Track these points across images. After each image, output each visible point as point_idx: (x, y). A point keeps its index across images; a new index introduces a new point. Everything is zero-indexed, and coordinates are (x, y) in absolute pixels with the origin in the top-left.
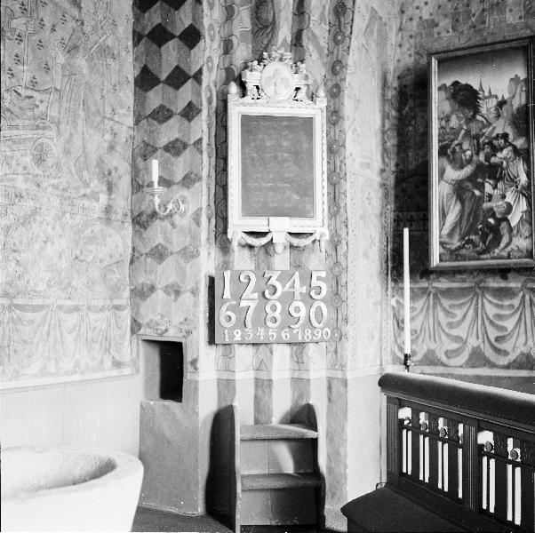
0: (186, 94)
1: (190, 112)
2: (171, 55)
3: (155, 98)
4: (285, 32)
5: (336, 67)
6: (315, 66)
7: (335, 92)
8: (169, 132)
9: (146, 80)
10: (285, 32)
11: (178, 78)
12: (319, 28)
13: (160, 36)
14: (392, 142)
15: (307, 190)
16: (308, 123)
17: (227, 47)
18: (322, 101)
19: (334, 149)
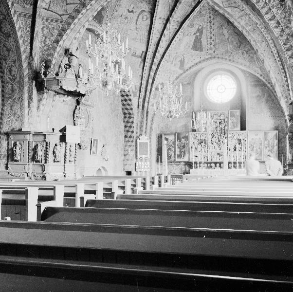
0: (131, 139)
1: (132, 141)
2: (129, 134)
3: (127, 139)
4: (144, 131)
5: (150, 135)
6: (148, 135)
7: (150, 139)
8: (129, 143)
9: (126, 137)
10: (144, 131)
11: (130, 137)
12: (148, 131)
13: (128, 131)
14: (157, 144)
15: (147, 152)
16: (147, 143)
17: (137, 133)
18: (149, 140)
19: (150, 145)
